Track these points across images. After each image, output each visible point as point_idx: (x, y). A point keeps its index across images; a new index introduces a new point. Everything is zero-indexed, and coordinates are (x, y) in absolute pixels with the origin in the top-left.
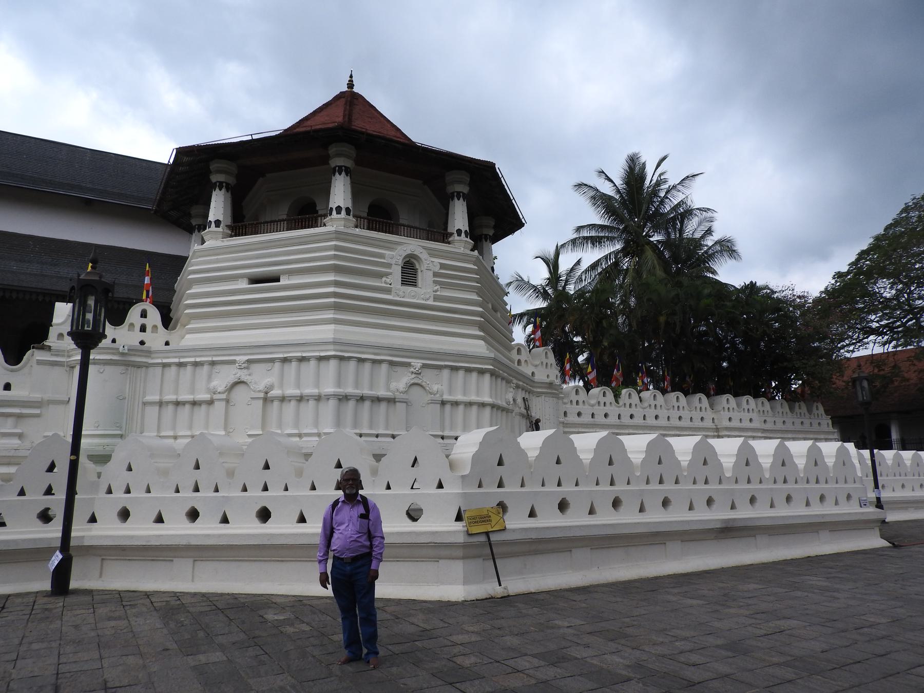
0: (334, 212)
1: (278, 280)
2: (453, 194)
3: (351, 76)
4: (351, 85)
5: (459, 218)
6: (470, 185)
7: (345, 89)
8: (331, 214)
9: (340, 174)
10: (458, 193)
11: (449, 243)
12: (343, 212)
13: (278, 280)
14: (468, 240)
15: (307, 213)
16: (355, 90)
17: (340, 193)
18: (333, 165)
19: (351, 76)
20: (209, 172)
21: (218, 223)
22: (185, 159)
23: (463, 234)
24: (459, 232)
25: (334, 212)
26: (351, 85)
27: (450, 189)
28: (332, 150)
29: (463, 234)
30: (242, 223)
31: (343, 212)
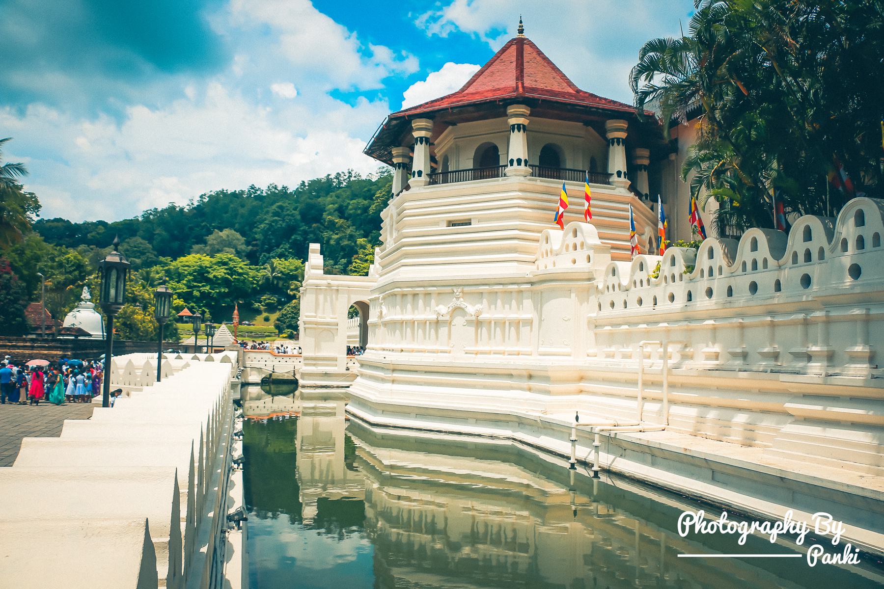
0: (515, 163)
1: (470, 224)
2: (613, 139)
3: (521, 22)
4: (521, 31)
5: (618, 161)
6: (627, 130)
7: (516, 35)
8: (512, 165)
9: (519, 131)
10: (618, 139)
11: (609, 183)
12: (523, 163)
13: (470, 224)
14: (626, 180)
15: (488, 164)
16: (526, 35)
17: (517, 147)
18: (511, 123)
19: (521, 22)
20: (411, 129)
21: (420, 173)
22: (394, 122)
23: (623, 175)
24: (619, 174)
25: (515, 163)
26: (521, 31)
27: (611, 135)
28: (511, 110)
29: (623, 175)
30: (439, 174)
31: (523, 163)
